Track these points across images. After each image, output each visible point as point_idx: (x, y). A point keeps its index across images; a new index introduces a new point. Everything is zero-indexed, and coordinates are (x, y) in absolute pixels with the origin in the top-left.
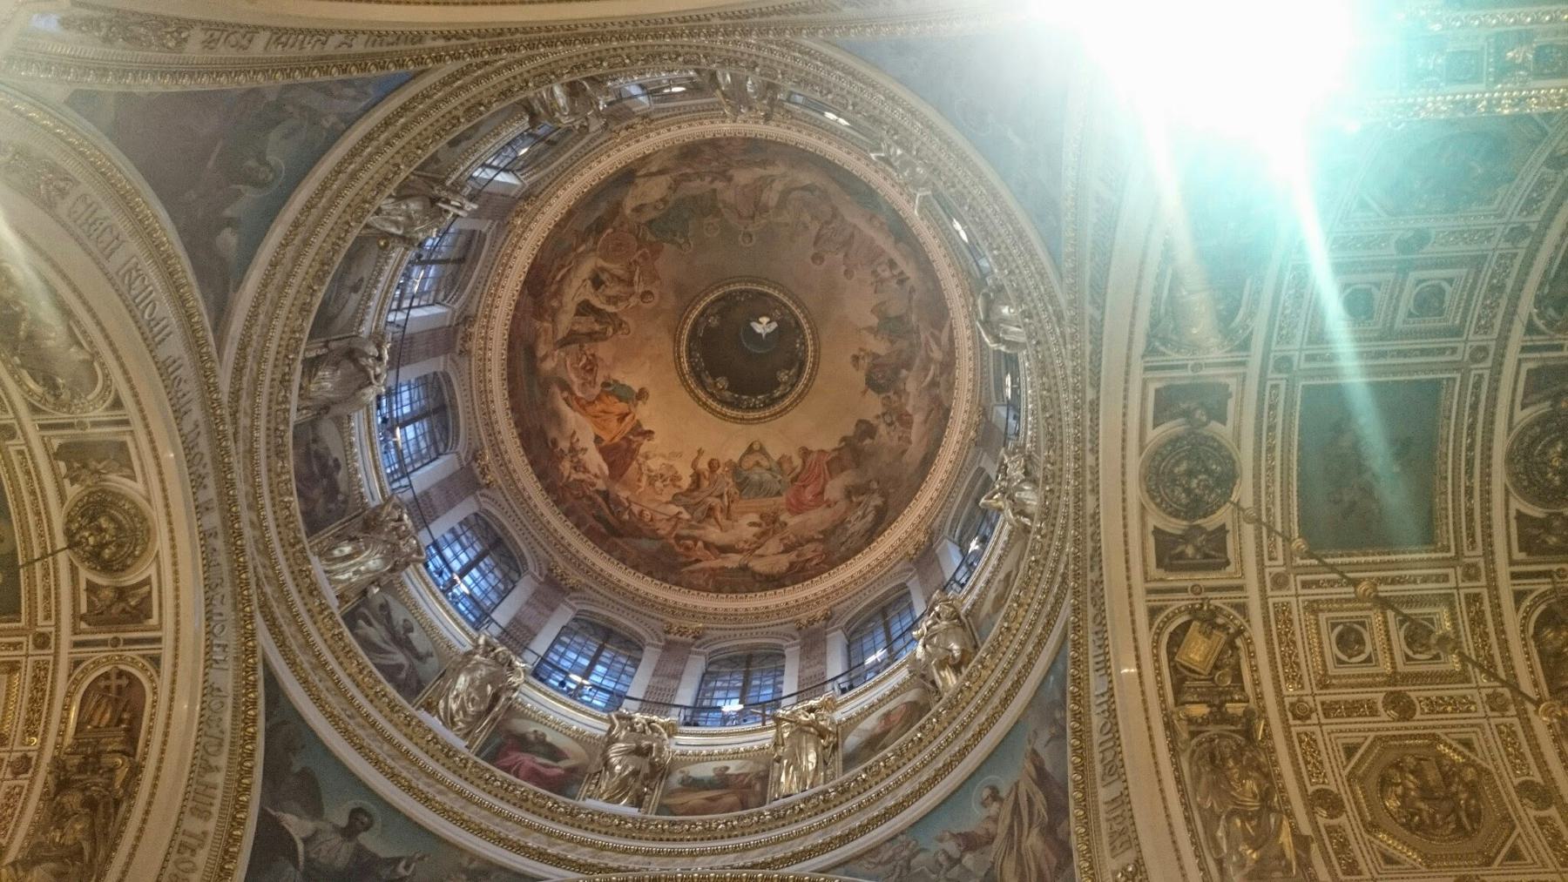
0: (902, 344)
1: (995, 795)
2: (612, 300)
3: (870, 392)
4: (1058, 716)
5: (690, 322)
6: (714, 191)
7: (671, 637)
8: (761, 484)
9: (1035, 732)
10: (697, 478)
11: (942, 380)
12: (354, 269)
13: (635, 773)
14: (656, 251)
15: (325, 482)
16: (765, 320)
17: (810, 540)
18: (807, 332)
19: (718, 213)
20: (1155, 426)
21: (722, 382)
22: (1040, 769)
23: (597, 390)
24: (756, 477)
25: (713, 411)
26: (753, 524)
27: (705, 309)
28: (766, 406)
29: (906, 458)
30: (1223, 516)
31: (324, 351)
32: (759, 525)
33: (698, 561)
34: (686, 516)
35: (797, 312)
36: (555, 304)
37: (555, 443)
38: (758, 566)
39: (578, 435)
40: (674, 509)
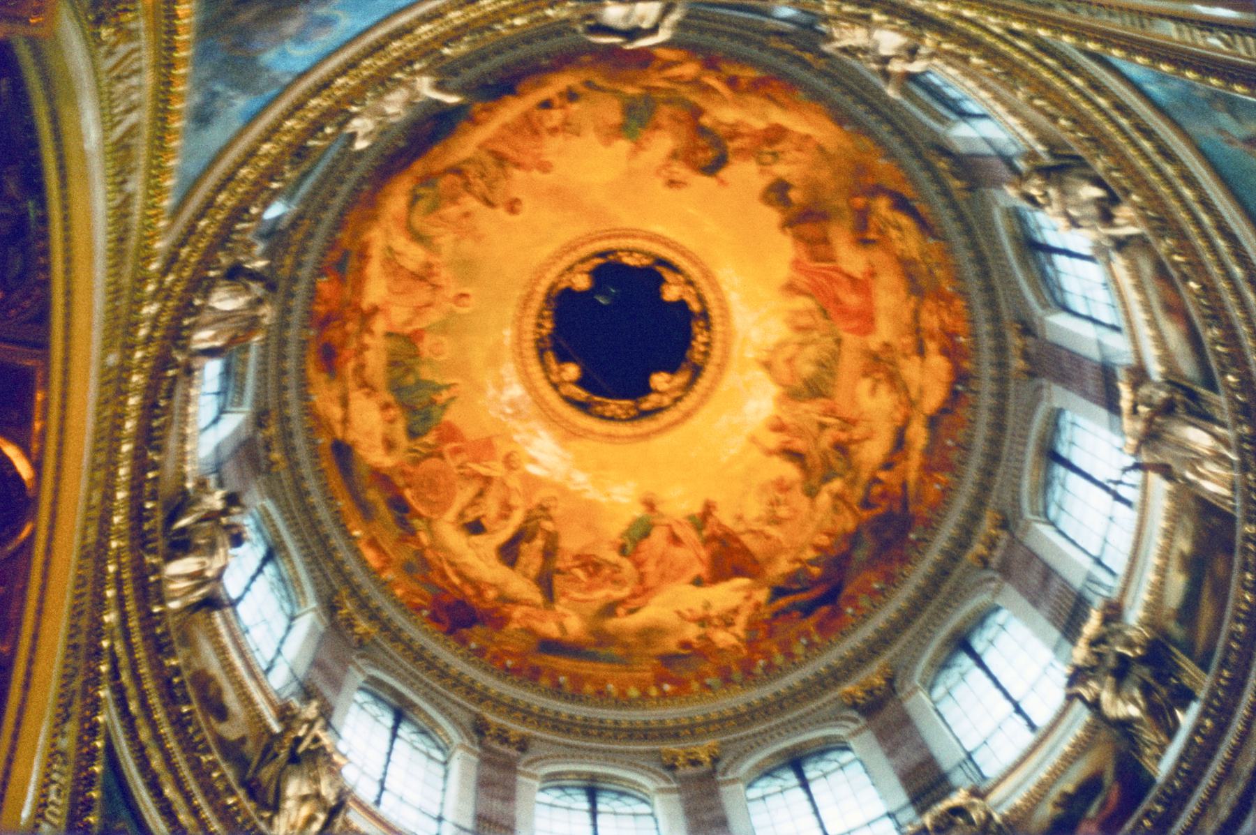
2: (506, 510)
3: (724, 173)
8: (820, 364)
14: (451, 433)
17: (916, 315)
21: (660, 380)
23: (627, 564)
29: (831, 147)
34: (836, 485)
36: (491, 594)
37: (686, 645)
38: (933, 399)
39: (682, 609)
40: (824, 499)
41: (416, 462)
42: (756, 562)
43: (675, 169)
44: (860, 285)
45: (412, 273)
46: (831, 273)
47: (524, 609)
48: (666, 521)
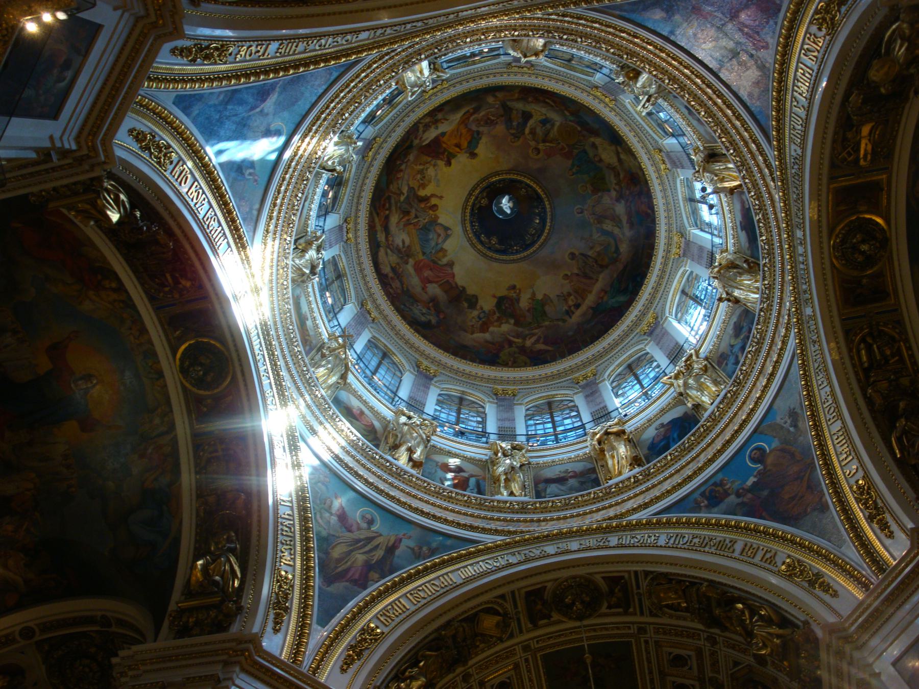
1: (371, 522)
2: (533, 132)
3: (495, 300)
4: (425, 549)
5: (522, 179)
6: (609, 191)
7: (345, 225)
8: (427, 241)
9: (410, 537)
10: (426, 199)
11: (513, 349)
13: (304, 274)
16: (511, 204)
17: (402, 284)
19: (596, 190)
20: (603, 578)
21: (484, 202)
23: (474, 128)
25: (467, 200)
26: (403, 242)
27: (531, 187)
30: (556, 616)
32: (404, 247)
33: (378, 214)
34: (402, 198)
35: (537, 246)
40: (405, 190)
44: (426, 281)
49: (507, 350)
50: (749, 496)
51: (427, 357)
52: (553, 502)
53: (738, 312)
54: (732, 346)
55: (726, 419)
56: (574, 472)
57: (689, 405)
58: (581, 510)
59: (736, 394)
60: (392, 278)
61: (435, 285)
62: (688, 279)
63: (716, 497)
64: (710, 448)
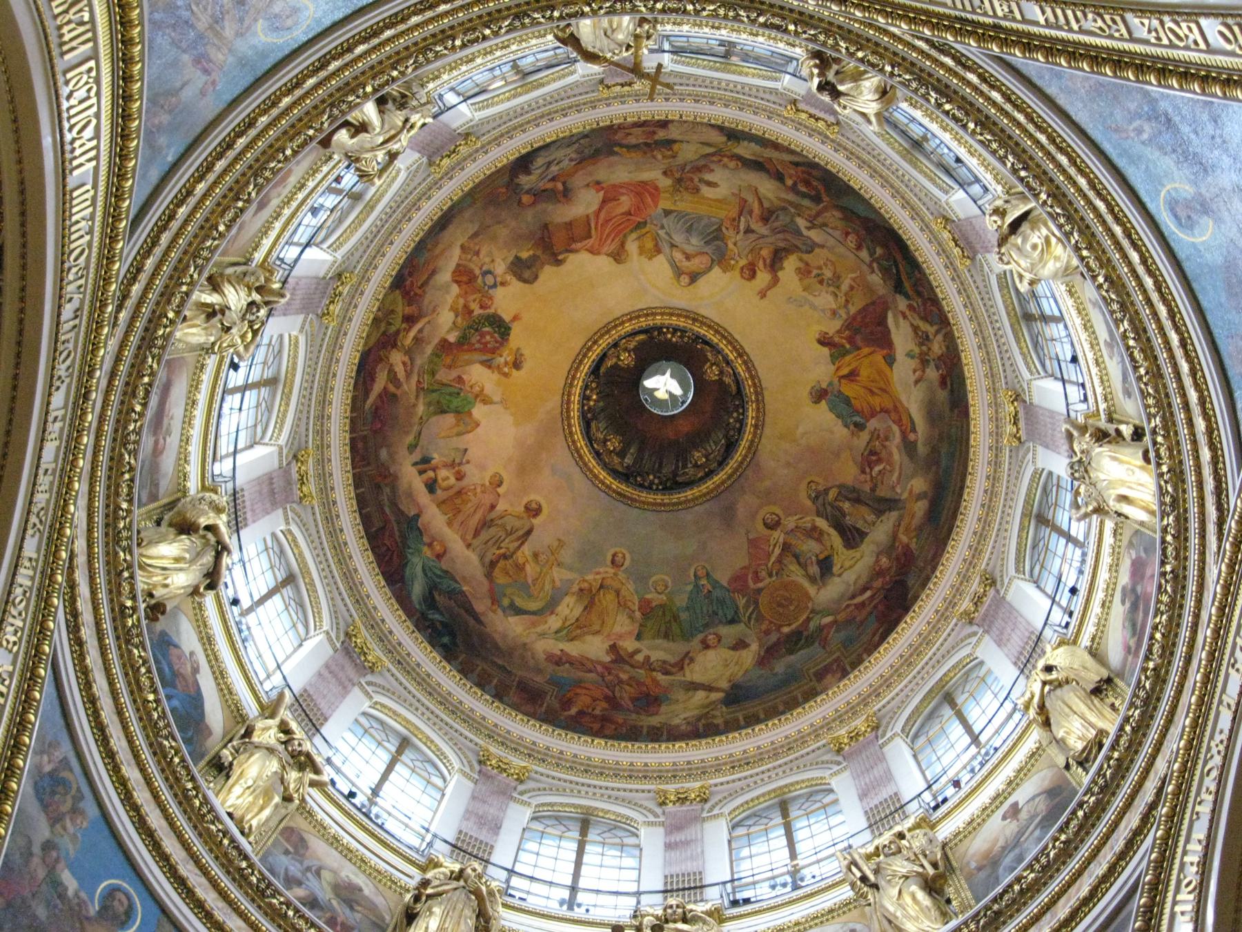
0: (444, 375)
2: (814, 533)
3: (507, 317)
4: (165, 118)
5: (728, 469)
6: (639, 637)
8: (689, 230)
9: (203, 93)
11: (398, 323)
12: (1001, 843)
14: (739, 580)
15: (1139, 589)
16: (661, 395)
17: (630, 147)
18: (575, 414)
19: (647, 610)
22: (201, 61)
23: (873, 424)
24: (694, 241)
25: (732, 342)
26: (710, 184)
27: (702, 480)
28: (659, 329)
31: (1071, 761)
32: (701, 180)
33: (797, 164)
34: (801, 223)
35: (581, 443)
37: (943, 383)
39: (913, 378)
40: (815, 235)
41: (761, 618)
42: (873, 303)
43: (502, 360)
44: (610, 195)
45: (586, 608)
46: (600, 222)
47: (902, 529)
48: (836, 381)
49: (401, 308)
50: (41, 873)
51: (472, 157)
52: (141, 415)
53: (379, 901)
54: (318, 873)
55: (198, 847)
56: (162, 452)
57: (227, 754)
58: (101, 473)
59: (241, 878)
60: (654, 133)
61: (595, 207)
62: (430, 761)
63: (53, 793)
64: (148, 795)
